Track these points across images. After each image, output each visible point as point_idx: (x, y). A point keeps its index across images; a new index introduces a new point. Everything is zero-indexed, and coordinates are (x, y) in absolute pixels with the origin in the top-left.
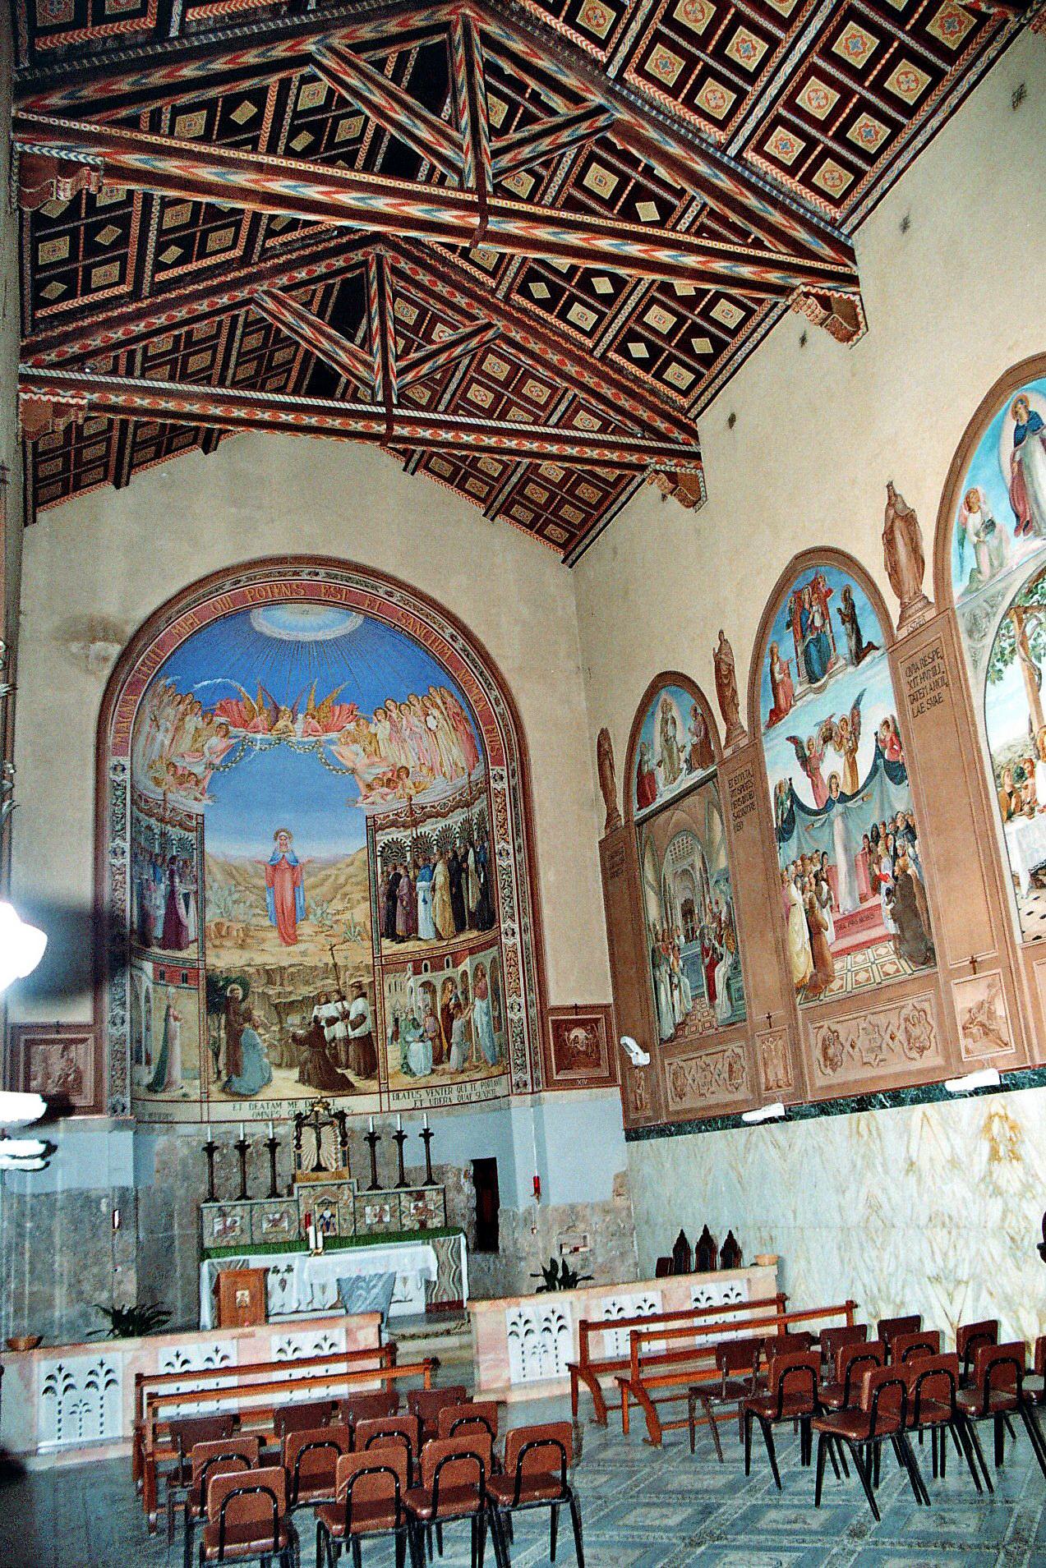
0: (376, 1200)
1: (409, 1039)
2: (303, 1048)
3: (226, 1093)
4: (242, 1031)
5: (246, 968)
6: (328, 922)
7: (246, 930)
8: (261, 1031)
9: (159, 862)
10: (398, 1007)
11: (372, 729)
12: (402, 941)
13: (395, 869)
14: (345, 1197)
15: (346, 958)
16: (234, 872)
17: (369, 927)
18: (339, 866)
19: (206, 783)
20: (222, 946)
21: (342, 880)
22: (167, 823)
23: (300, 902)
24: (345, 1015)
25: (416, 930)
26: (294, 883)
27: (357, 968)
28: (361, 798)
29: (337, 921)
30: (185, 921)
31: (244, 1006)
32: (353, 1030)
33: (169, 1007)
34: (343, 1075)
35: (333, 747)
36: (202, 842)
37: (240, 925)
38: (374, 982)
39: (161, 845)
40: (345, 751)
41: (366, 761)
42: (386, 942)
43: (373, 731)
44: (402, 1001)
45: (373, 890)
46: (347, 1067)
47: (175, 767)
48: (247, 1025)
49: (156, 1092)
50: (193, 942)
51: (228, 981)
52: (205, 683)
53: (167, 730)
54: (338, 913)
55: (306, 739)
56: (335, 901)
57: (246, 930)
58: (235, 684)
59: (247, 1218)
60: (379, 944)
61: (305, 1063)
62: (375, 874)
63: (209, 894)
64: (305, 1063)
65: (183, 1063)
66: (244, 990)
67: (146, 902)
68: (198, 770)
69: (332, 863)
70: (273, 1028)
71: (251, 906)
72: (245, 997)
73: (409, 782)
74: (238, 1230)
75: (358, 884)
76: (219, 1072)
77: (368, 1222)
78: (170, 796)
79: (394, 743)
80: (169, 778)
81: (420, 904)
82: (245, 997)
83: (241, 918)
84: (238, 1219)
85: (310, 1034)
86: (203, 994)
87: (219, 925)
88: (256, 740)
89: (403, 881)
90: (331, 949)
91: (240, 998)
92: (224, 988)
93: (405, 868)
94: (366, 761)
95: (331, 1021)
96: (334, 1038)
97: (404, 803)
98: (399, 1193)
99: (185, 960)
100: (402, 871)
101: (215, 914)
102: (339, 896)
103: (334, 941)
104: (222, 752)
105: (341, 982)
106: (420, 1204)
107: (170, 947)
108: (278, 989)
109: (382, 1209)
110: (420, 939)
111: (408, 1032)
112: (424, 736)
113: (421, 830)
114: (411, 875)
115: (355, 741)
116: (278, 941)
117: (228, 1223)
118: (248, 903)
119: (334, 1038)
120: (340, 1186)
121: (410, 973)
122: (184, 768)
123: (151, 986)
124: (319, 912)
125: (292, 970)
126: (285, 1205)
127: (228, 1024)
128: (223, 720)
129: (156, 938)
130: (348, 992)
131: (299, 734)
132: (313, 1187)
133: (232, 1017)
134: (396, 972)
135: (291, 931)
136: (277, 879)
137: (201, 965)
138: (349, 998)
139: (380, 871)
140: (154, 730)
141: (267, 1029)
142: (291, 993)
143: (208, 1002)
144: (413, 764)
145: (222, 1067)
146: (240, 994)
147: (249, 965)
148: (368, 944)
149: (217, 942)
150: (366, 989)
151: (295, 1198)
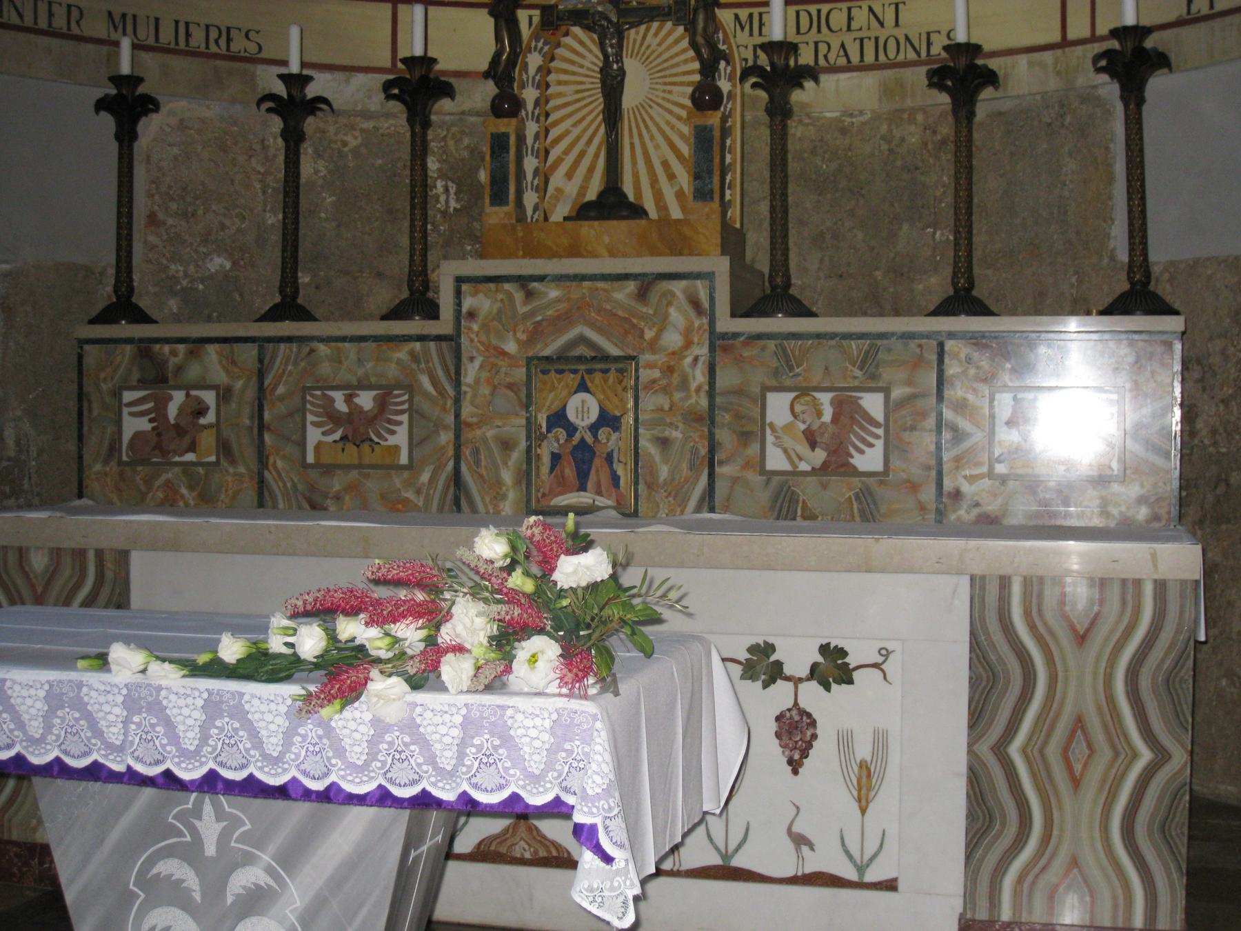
14: (672, 339)
74: (207, 440)
77: (776, 460)
84: (209, 397)
117: (172, 411)
120: (646, 284)
126: (402, 354)
151: (444, 325)
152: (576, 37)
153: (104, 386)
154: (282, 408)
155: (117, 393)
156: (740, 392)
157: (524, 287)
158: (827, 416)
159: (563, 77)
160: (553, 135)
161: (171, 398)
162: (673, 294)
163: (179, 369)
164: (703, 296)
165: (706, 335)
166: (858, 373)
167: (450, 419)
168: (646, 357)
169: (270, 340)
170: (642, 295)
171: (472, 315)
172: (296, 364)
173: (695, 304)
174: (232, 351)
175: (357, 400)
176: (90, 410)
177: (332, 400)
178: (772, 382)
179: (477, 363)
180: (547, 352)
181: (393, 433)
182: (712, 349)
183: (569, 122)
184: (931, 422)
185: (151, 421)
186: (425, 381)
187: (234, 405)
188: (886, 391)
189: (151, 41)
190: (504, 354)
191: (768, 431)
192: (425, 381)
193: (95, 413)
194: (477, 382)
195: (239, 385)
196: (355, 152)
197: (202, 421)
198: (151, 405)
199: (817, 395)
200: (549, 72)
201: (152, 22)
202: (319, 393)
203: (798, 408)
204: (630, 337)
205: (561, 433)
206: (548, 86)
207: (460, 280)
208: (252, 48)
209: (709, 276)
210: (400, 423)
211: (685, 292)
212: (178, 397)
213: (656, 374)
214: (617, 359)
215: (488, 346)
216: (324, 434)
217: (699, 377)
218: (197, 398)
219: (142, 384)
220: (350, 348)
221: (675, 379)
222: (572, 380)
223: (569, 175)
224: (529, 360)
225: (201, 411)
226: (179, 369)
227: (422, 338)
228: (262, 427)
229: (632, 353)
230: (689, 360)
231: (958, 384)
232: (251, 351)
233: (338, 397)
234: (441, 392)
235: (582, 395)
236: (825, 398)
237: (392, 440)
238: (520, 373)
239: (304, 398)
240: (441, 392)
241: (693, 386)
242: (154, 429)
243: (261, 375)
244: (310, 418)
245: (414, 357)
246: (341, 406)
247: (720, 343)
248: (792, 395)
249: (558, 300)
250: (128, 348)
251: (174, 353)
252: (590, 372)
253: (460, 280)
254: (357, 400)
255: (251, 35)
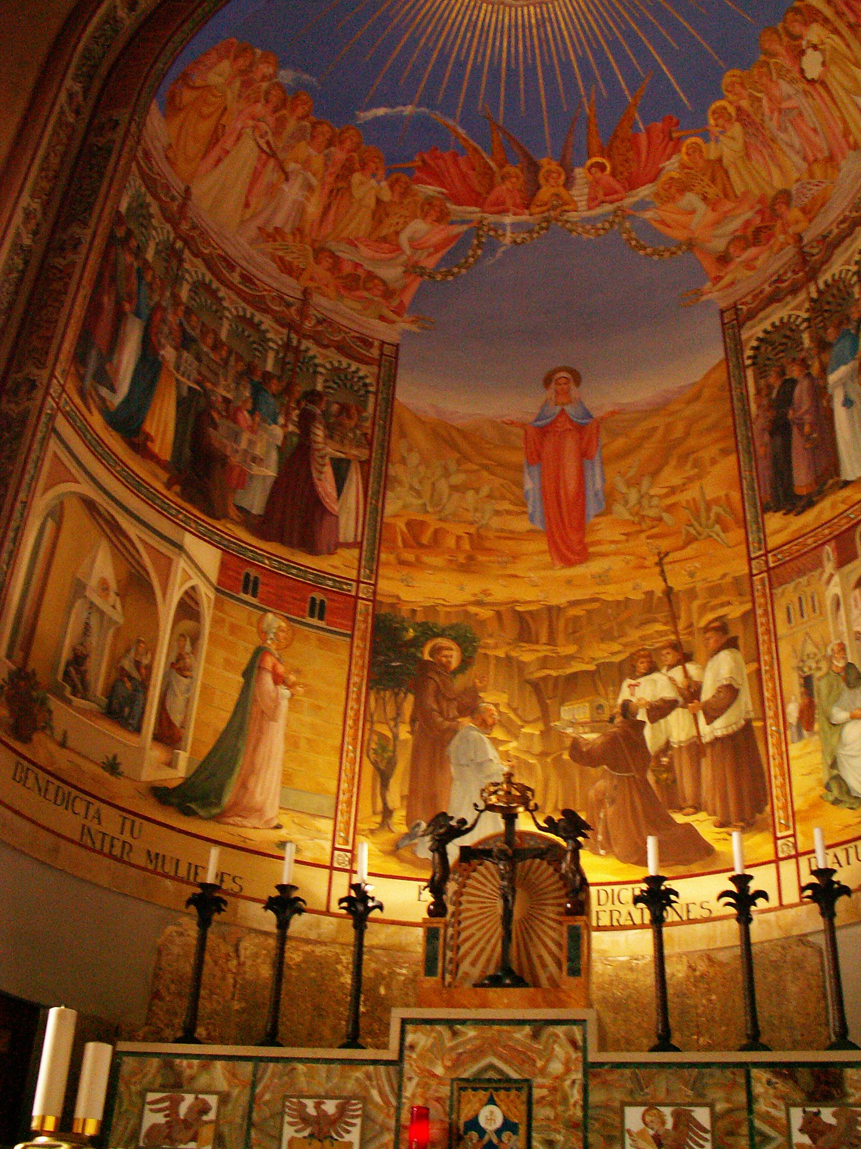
0: (661, 1084)
1: (840, 715)
2: (592, 770)
3: (401, 860)
4: (454, 731)
5: (473, 609)
6: (652, 513)
7: (478, 541)
8: (498, 733)
9: (275, 386)
10: (810, 648)
11: (712, 153)
12: (810, 504)
13: (783, 373)
14: (556, 1067)
15: (692, 575)
16: (459, 440)
17: (738, 506)
18: (673, 407)
19: (407, 298)
20: (418, 565)
21: (679, 432)
22: (308, 337)
23: (595, 482)
24: (691, 692)
25: (835, 466)
26: (584, 454)
27: (714, 591)
28: (709, 284)
29: (670, 509)
30: (330, 501)
31: (459, 683)
32: (710, 720)
33: (260, 653)
34: (689, 827)
35: (648, 215)
36: (390, 382)
37: (460, 530)
38: (753, 610)
39: (281, 363)
40: (668, 212)
41: (711, 216)
42: (774, 521)
43: (713, 156)
44: (817, 637)
45: (740, 431)
46: (697, 808)
47: (337, 262)
48: (466, 722)
49: (188, 812)
50: (348, 546)
51: (428, 631)
52: (381, 111)
53: (310, 188)
54: (673, 491)
55: (599, 211)
56: (667, 472)
57: (478, 541)
58: (437, 116)
59: (240, 1095)
60: (761, 528)
61: (600, 803)
62: (745, 400)
63: (395, 470)
64: (600, 803)
65: (287, 778)
66: (463, 651)
67: (219, 437)
68: (391, 273)
69: (660, 407)
70: (527, 730)
71: (490, 496)
72: (466, 663)
73: (794, 213)
75: (708, 430)
76: (387, 813)
78: (317, 299)
79: (754, 155)
80: (321, 271)
81: (841, 415)
82: (466, 663)
83: (470, 516)
84: (213, 1100)
85: (612, 742)
86: (361, 647)
87: (416, 527)
88: (503, 226)
89: (801, 391)
90: (660, 563)
91: (455, 663)
92: (417, 643)
93: (804, 364)
94: (711, 216)
95: (660, 710)
96: (668, 745)
97: (790, 251)
98: (745, 1067)
99: (321, 575)
100: (794, 372)
101: (405, 507)
102: (673, 462)
103: (664, 544)
104: (437, 248)
105: (681, 625)
106: (827, 1115)
107: (281, 538)
108: (544, 650)
109: (683, 1120)
110: (847, 484)
111: (836, 701)
112: (804, 103)
113: (826, 277)
114: (815, 369)
115: (684, 188)
116: (547, 558)
117: (183, 1109)
118: (485, 491)
119: (668, 745)
120: (539, 1026)
121: (829, 567)
122: (357, 265)
123: (207, 594)
124: (633, 496)
125: (572, 612)
127: (420, 718)
128: (431, 190)
129: (240, 509)
130: (698, 644)
131: (582, 204)
132: (450, 1023)
133: (431, 703)
134: (801, 573)
135: (574, 537)
136: (548, 449)
137: (364, 591)
138: (700, 653)
139: (752, 390)
140: (270, 174)
141: (513, 731)
142: (571, 658)
143: (372, 664)
144: (796, 175)
145: (395, 797)
146: (454, 658)
147: (479, 603)
148: (737, 534)
149: (409, 556)
150: (736, 631)
151: (391, 1054)
152: (487, 868)
153: (133, 1088)
154: (267, 1112)
155: (142, 1095)
156: (606, 1107)
157: (451, 1028)
158: (669, 1125)
159: (471, 898)
160: (463, 935)
161: (183, 1099)
162: (557, 1036)
163: (192, 1078)
164: (578, 1037)
165: (580, 1065)
166: (690, 1093)
167: (392, 1123)
168: (539, 1080)
169: (261, 1059)
170: (535, 1036)
171: (412, 1047)
172: (280, 1078)
173: (573, 1043)
174: (234, 1067)
175: (323, 1107)
176: (120, 1107)
177: (305, 1106)
178: (628, 1099)
179: (415, 1080)
180: (465, 1075)
181: (348, 1132)
182: (585, 1074)
183: (475, 928)
184: (744, 1130)
185: (166, 1116)
186: (375, 1093)
187: (230, 1106)
188: (711, 1106)
189: (172, 874)
190: (434, 1075)
191: (627, 1135)
192: (375, 1093)
193: (124, 1108)
194: (414, 1095)
195: (236, 1092)
196: (298, 965)
197: (205, 1118)
198: (167, 1104)
199: (662, 1109)
200: (462, 894)
201: (174, 861)
202: (295, 1100)
203: (648, 1118)
204: (527, 1066)
205: (474, 1135)
206: (460, 903)
207: (404, 1022)
208: (237, 889)
209: (581, 1022)
210: (354, 1125)
211: (566, 1034)
212: (189, 1099)
213: (545, 1092)
214: (516, 1081)
215: (422, 1070)
216: (296, 1131)
217: (576, 1095)
218: (203, 1100)
219: (163, 1088)
220: (323, 1068)
221: (558, 1097)
222: (482, 1095)
223: (473, 964)
224: (453, 1080)
225: (205, 1110)
226: (192, 1078)
227: (375, 1062)
228: (251, 1124)
229: (527, 1076)
230: (568, 1083)
231: (761, 1100)
232: (249, 1067)
233: (310, 1104)
234: (387, 1102)
235: (492, 1107)
236: (667, 1111)
237: (347, 1138)
238: (445, 1091)
239: (284, 1106)
240: (387, 1102)
241: (572, 1101)
242: (167, 1122)
243: (254, 1085)
244: (287, 1119)
245: (368, 1077)
246: (311, 1110)
247: (590, 1069)
248: (643, 1109)
249: (475, 1038)
250: (155, 1062)
251: (190, 1066)
252: (496, 1089)
253: (404, 1022)
254: (323, 1107)
255: (237, 880)
